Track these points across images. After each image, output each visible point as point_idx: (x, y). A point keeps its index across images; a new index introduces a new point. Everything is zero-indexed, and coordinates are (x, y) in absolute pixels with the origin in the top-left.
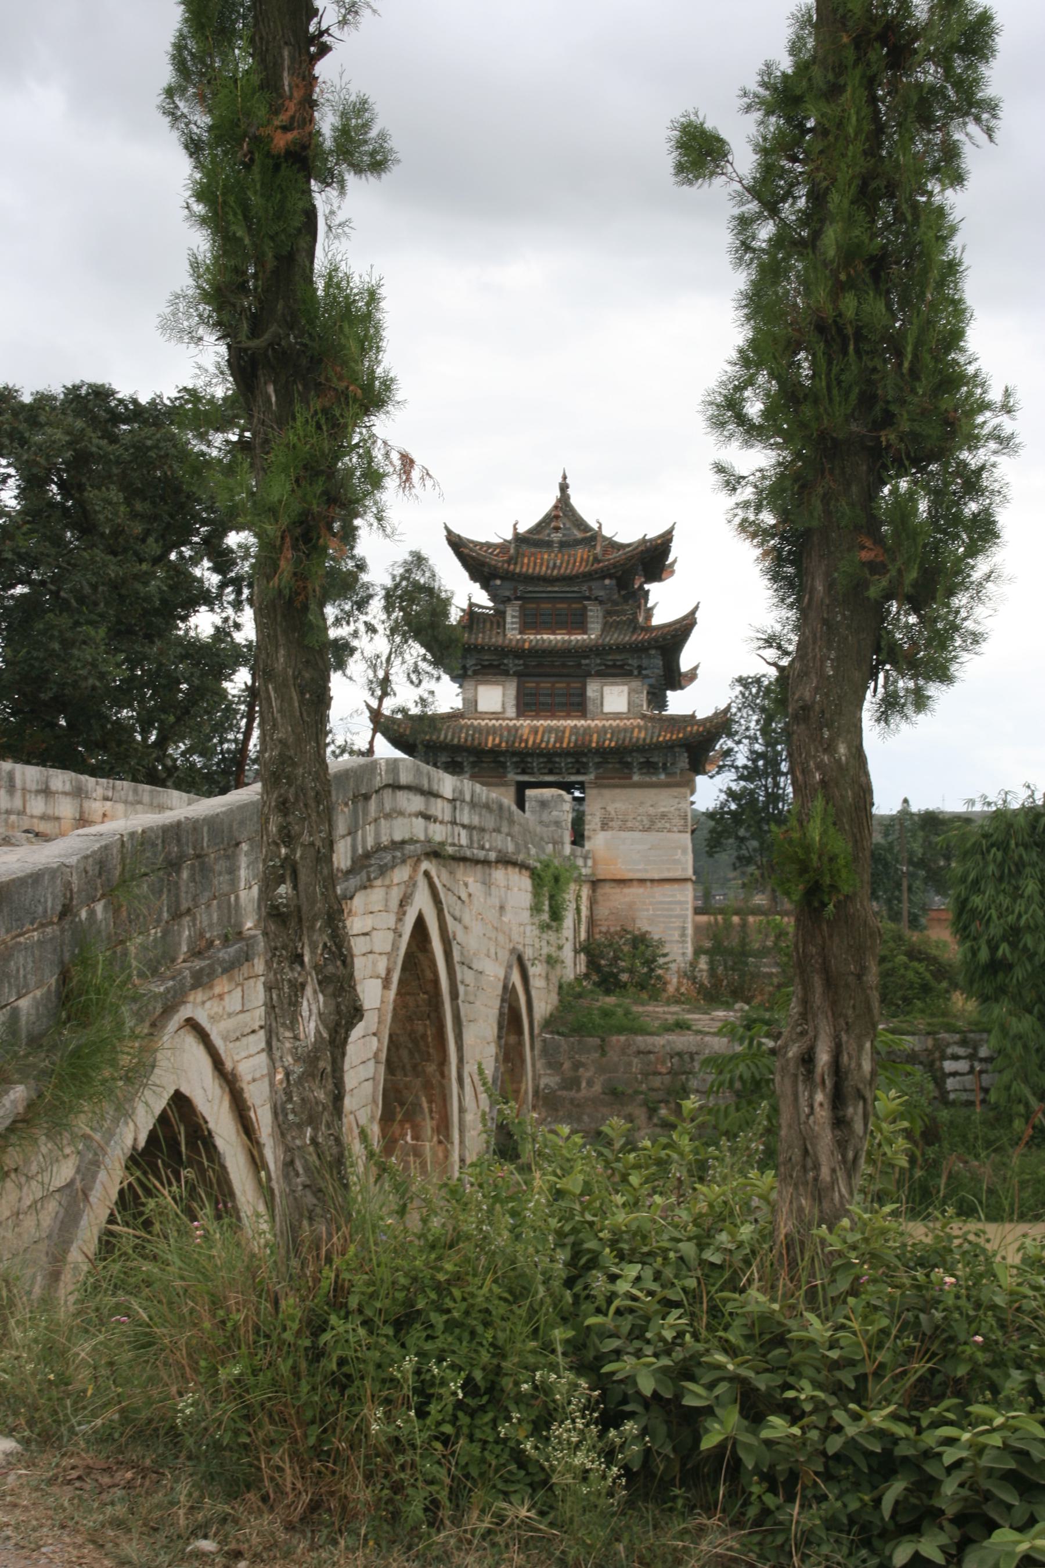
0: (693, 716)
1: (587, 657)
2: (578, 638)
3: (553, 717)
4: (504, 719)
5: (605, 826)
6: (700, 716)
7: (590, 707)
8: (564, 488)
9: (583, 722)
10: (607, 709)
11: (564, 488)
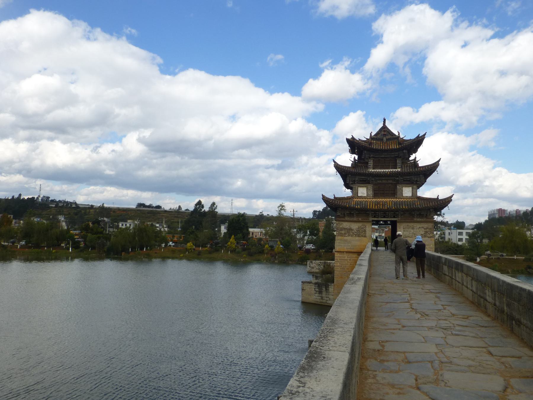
1: (398, 177)
4: (368, 199)
6: (440, 198)
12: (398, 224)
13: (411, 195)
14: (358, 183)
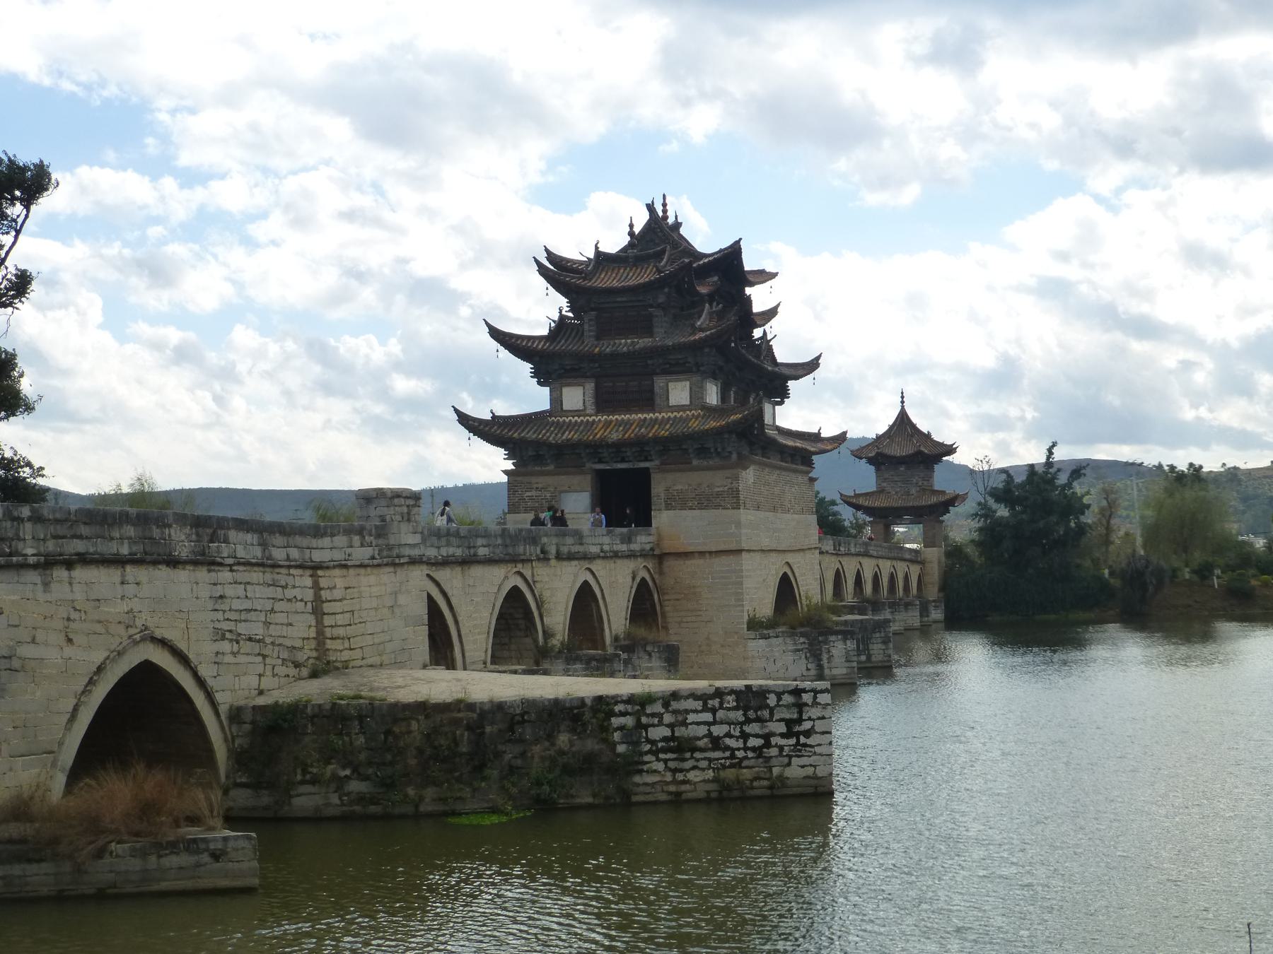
2: (643, 342)
3: (629, 411)
4: (585, 416)
5: (668, 507)
7: (658, 401)
9: (651, 415)
10: (672, 402)
12: (653, 475)
13: (688, 402)
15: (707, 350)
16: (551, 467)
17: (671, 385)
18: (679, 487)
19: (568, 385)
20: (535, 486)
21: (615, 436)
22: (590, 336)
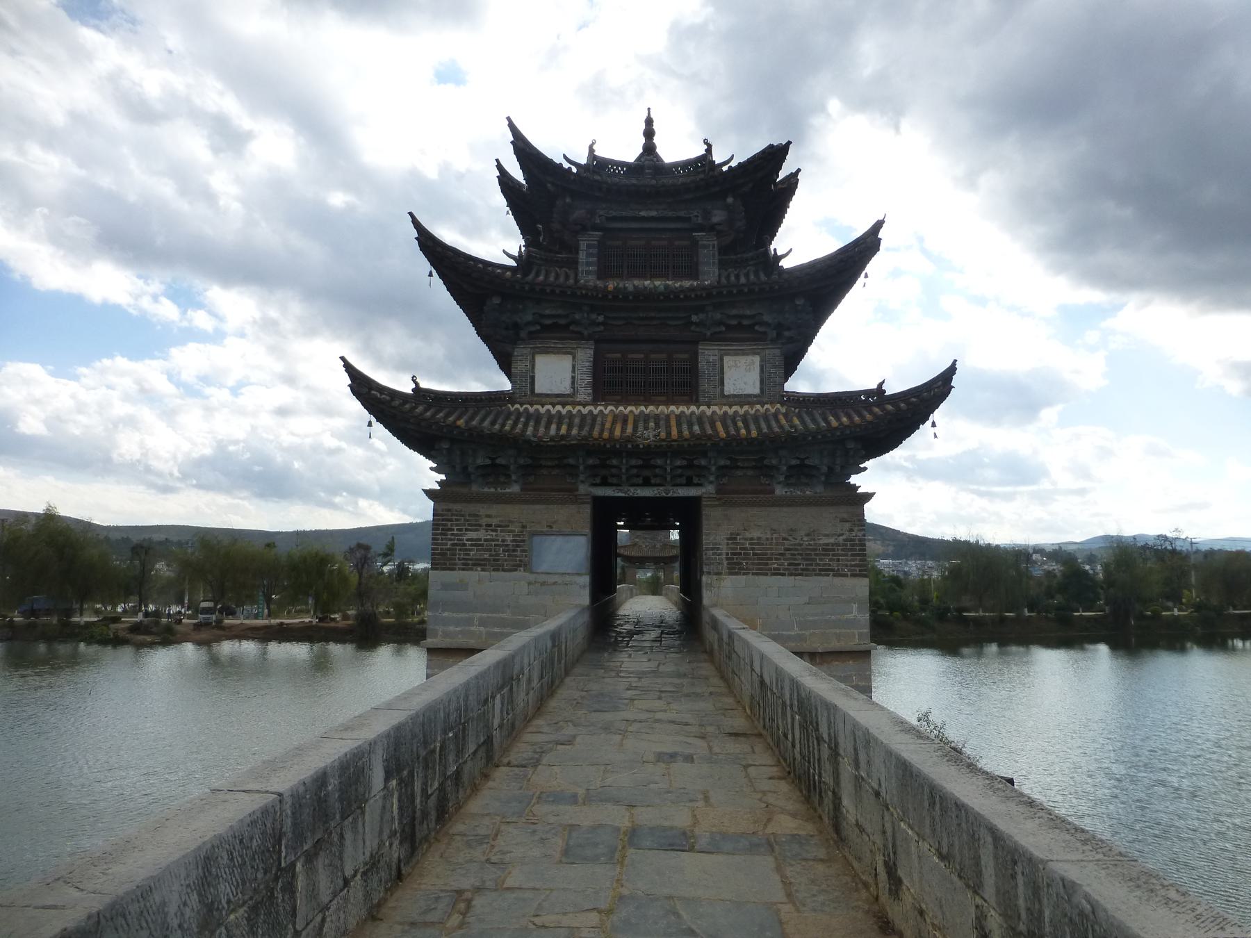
0: (880, 390)
3: (647, 402)
4: (574, 404)
6: (892, 389)
7: (704, 385)
8: (649, 133)
9: (693, 408)
10: (729, 389)
11: (649, 133)
12: (706, 512)
13: (757, 391)
14: (532, 336)
15: (800, 302)
16: (515, 488)
17: (728, 360)
18: (755, 534)
19: (546, 351)
20: (484, 521)
21: (648, 435)
22: (588, 273)
